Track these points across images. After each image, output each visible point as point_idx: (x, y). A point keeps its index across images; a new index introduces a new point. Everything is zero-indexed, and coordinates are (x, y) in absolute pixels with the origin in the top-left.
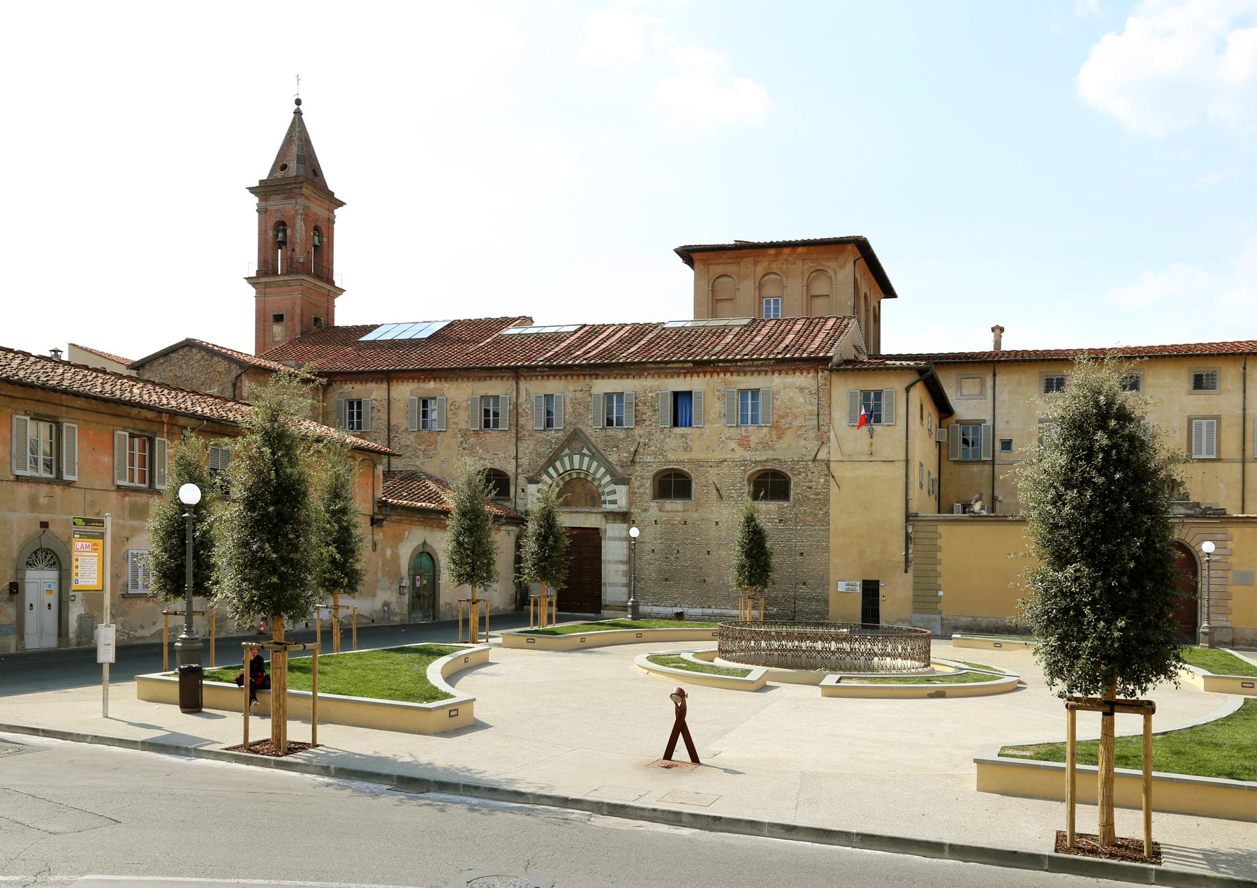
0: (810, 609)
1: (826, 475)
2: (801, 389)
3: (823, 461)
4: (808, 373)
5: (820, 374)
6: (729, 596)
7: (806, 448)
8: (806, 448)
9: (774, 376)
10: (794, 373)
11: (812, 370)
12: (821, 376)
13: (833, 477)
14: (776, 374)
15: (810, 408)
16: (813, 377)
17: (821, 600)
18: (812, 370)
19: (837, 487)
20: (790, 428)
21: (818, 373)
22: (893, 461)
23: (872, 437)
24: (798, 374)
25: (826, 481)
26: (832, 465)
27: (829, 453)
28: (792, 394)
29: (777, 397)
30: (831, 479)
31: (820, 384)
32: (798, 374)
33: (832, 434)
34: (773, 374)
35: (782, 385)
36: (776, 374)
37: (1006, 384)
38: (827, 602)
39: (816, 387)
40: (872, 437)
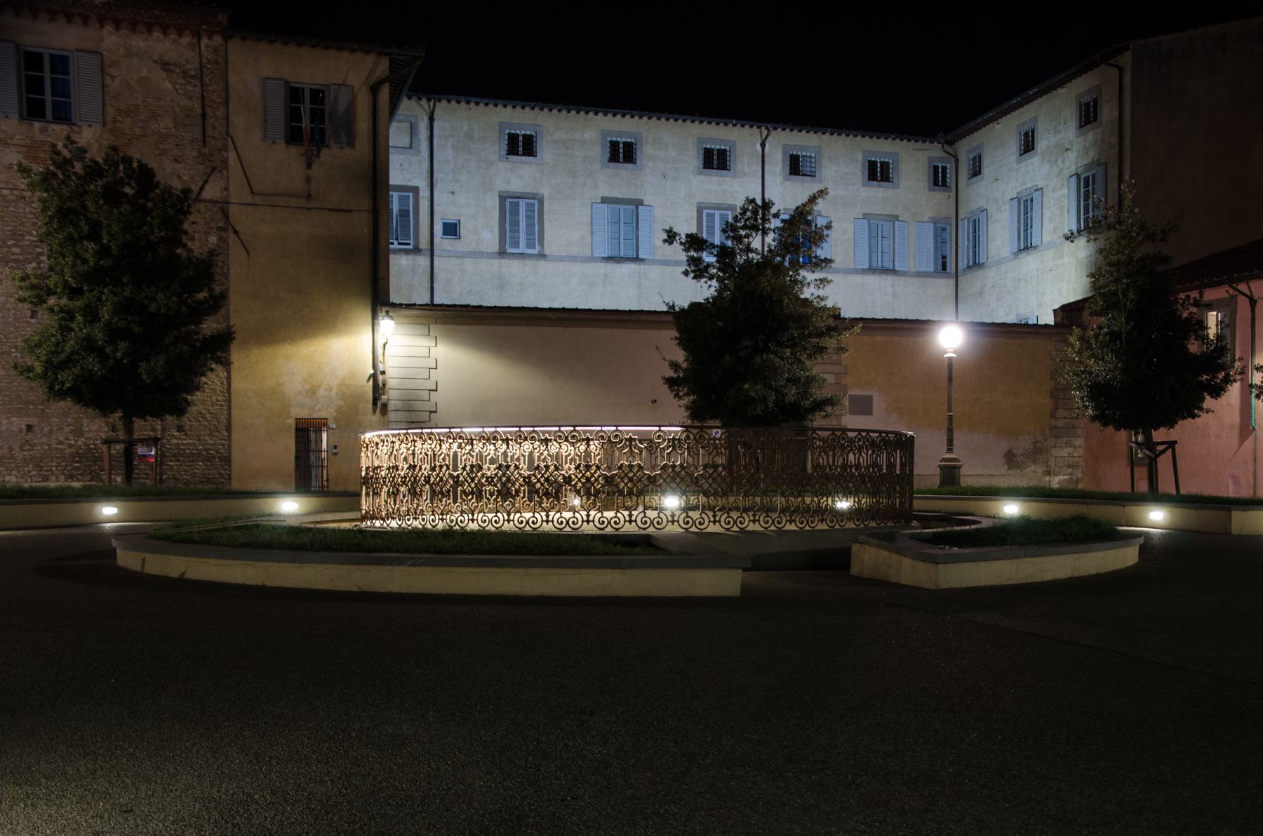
0: (193, 475)
1: (220, 229)
2: (165, 65)
3: (213, 202)
4: (180, 35)
5: (205, 41)
6: (12, 457)
7: (180, 177)
8: (180, 177)
9: (104, 31)
10: (150, 32)
11: (187, 32)
12: (207, 46)
13: (236, 232)
14: (109, 28)
15: (185, 103)
16: (189, 44)
17: (215, 458)
18: (187, 32)
19: (244, 252)
20: (144, 136)
21: (199, 39)
22: (350, 211)
23: (309, 166)
24: (157, 35)
25: (220, 238)
26: (234, 210)
27: (226, 189)
28: (145, 70)
29: (113, 71)
30: (232, 238)
31: (205, 61)
32: (157, 35)
33: (232, 155)
34: (102, 26)
35: (122, 51)
36: (109, 28)
37: (451, 136)
38: (227, 460)
39: (197, 65)
40: (309, 166)
